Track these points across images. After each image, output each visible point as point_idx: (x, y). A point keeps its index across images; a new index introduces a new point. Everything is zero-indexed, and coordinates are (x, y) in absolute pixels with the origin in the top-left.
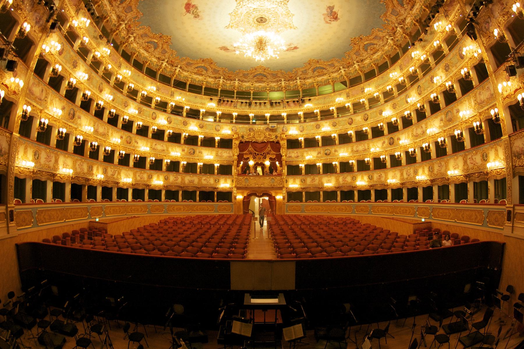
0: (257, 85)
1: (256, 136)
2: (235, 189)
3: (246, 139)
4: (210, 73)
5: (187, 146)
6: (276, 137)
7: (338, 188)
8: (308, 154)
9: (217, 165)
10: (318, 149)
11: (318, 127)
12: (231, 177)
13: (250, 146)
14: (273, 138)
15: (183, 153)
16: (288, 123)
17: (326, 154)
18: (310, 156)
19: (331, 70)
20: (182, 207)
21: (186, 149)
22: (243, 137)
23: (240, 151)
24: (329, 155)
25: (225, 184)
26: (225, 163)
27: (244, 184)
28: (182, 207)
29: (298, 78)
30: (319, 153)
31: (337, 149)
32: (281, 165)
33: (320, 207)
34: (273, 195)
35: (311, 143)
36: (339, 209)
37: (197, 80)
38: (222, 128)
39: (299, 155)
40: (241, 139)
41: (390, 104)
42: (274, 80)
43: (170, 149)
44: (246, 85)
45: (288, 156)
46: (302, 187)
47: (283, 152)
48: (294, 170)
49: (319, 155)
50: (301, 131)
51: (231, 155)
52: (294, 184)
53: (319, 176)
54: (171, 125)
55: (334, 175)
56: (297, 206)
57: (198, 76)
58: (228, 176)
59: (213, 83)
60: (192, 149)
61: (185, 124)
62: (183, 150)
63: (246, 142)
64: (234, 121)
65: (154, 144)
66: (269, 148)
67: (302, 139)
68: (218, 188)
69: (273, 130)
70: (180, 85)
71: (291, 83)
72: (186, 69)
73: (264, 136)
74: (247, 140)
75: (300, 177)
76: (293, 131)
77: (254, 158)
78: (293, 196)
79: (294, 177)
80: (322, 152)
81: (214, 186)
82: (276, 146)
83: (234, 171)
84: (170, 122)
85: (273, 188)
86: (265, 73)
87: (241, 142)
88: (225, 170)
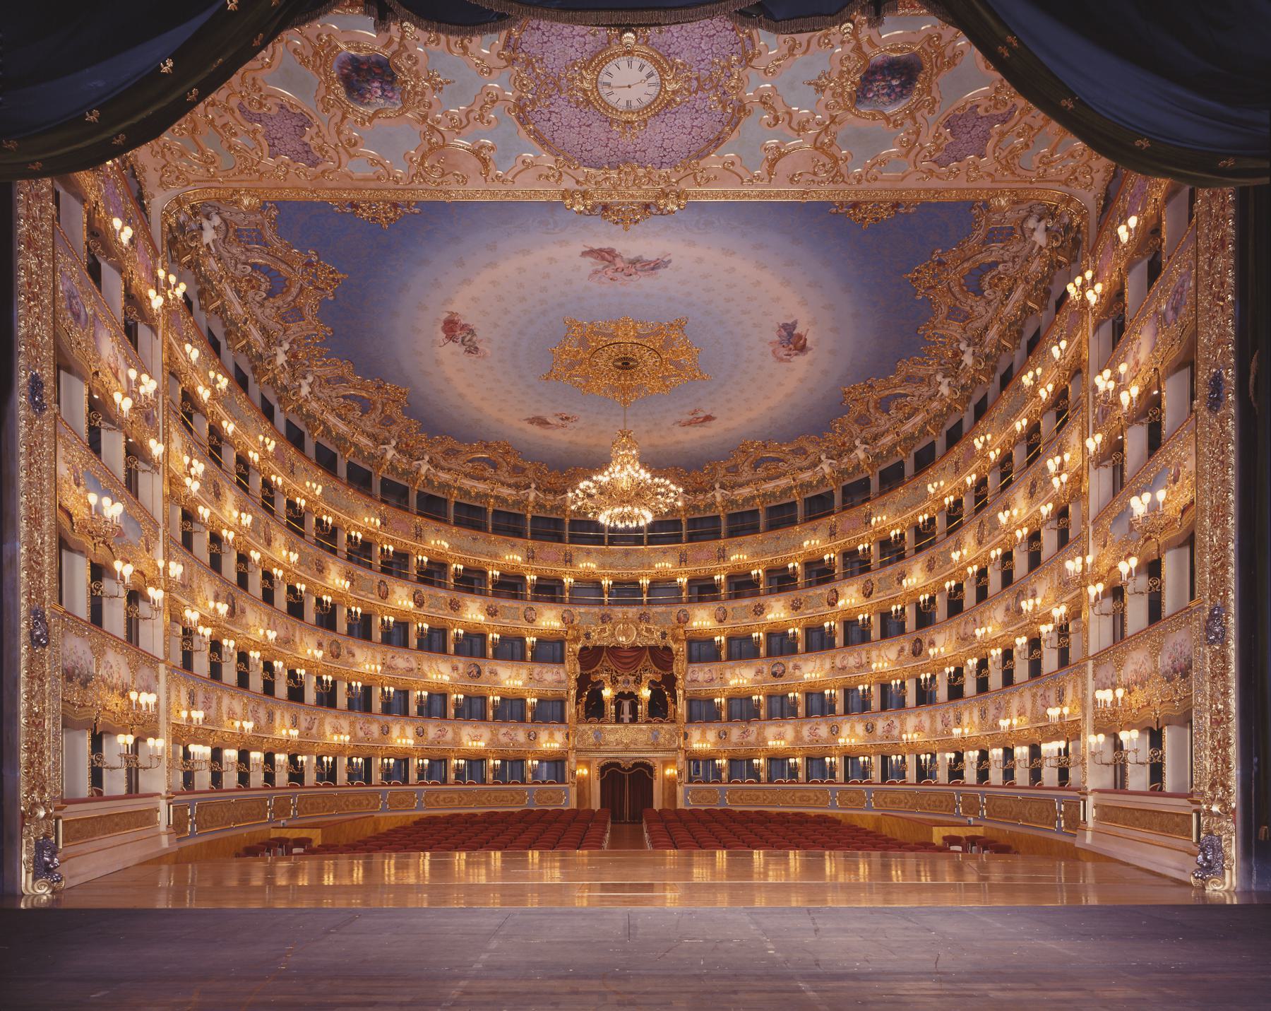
3: (596, 639)
4: (503, 475)
8: (733, 674)
10: (758, 663)
11: (759, 610)
15: (455, 675)
17: (774, 674)
18: (741, 677)
19: (799, 462)
20: (455, 796)
21: (461, 666)
22: (588, 636)
24: (781, 676)
28: (455, 796)
29: (717, 486)
30: (759, 672)
35: (741, 649)
36: (801, 799)
38: (542, 615)
41: (923, 558)
43: (425, 668)
47: (679, 667)
48: (702, 711)
49: (759, 678)
50: (720, 621)
54: (424, 611)
57: (475, 483)
60: (476, 665)
61: (455, 606)
62: (455, 669)
65: (389, 656)
70: (432, 507)
72: (443, 463)
75: (718, 725)
76: (702, 619)
80: (765, 670)
84: (419, 603)
88: (549, 711)
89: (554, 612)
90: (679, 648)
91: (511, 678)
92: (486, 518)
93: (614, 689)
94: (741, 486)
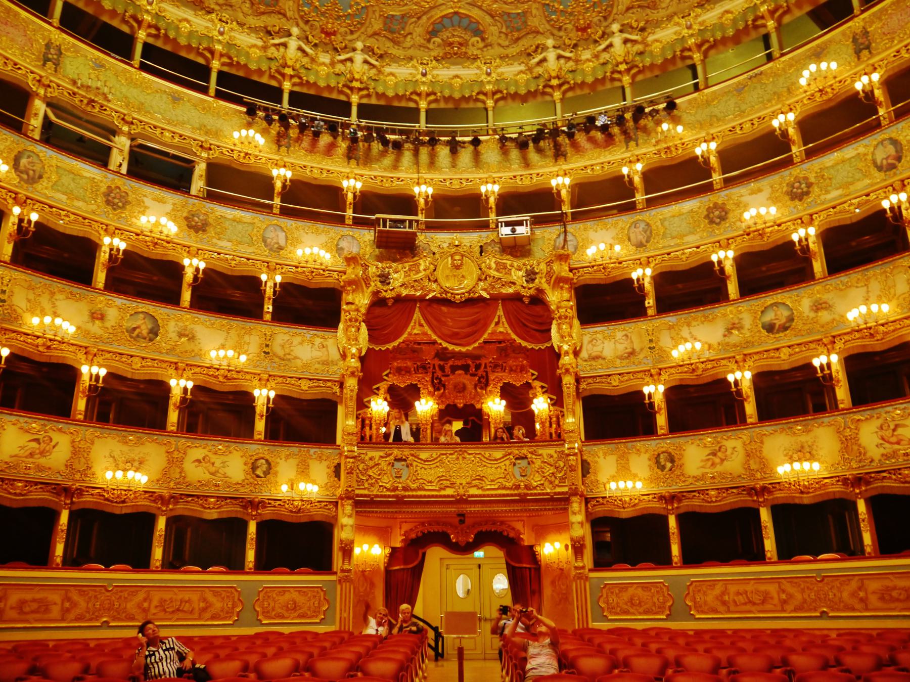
0: (444, 73)
1: (439, 274)
2: (348, 509)
5: (119, 301)
6: (531, 276)
7: (858, 481)
9: (263, 395)
10: (724, 313)
12: (328, 451)
13: (417, 315)
14: (516, 277)
16: (576, 217)
17: (770, 328)
23: (372, 338)
24: (784, 328)
25: (300, 483)
26: (305, 389)
27: (387, 481)
31: (826, 297)
32: (558, 401)
33: (772, 589)
34: (527, 539)
37: (185, 27)
39: (637, 347)
40: (375, 285)
42: (513, 50)
44: (399, 76)
45: (584, 354)
46: (664, 490)
47: (566, 334)
48: (616, 417)
50: (640, 245)
51: (335, 355)
52: (627, 479)
53: (745, 434)
55: (827, 419)
56: (645, 587)
58: (314, 450)
59: (256, 53)
61: (114, 200)
62: (97, 316)
63: (398, 299)
64: (349, 213)
66: (500, 326)
67: (643, 274)
68: (262, 504)
69: (516, 249)
71: (586, 55)
73: (476, 273)
74: (404, 292)
75: (650, 445)
76: (601, 246)
77: (438, 386)
78: (625, 539)
79: (622, 445)
80: (747, 321)
81: (245, 492)
82: (531, 313)
83: (346, 423)
85: (523, 500)
86: (475, 13)
87: (378, 302)
88: (304, 421)
89: (323, 238)
90: (559, 299)
91: (223, 349)
92: (207, 80)
93: (440, 399)
94: (657, 24)
